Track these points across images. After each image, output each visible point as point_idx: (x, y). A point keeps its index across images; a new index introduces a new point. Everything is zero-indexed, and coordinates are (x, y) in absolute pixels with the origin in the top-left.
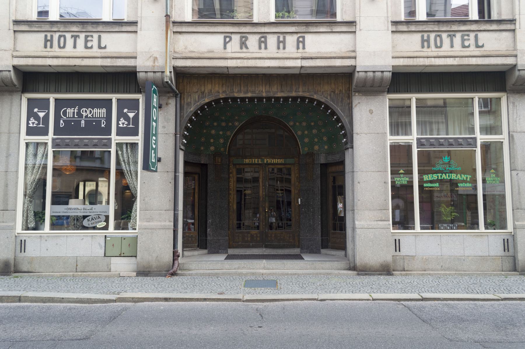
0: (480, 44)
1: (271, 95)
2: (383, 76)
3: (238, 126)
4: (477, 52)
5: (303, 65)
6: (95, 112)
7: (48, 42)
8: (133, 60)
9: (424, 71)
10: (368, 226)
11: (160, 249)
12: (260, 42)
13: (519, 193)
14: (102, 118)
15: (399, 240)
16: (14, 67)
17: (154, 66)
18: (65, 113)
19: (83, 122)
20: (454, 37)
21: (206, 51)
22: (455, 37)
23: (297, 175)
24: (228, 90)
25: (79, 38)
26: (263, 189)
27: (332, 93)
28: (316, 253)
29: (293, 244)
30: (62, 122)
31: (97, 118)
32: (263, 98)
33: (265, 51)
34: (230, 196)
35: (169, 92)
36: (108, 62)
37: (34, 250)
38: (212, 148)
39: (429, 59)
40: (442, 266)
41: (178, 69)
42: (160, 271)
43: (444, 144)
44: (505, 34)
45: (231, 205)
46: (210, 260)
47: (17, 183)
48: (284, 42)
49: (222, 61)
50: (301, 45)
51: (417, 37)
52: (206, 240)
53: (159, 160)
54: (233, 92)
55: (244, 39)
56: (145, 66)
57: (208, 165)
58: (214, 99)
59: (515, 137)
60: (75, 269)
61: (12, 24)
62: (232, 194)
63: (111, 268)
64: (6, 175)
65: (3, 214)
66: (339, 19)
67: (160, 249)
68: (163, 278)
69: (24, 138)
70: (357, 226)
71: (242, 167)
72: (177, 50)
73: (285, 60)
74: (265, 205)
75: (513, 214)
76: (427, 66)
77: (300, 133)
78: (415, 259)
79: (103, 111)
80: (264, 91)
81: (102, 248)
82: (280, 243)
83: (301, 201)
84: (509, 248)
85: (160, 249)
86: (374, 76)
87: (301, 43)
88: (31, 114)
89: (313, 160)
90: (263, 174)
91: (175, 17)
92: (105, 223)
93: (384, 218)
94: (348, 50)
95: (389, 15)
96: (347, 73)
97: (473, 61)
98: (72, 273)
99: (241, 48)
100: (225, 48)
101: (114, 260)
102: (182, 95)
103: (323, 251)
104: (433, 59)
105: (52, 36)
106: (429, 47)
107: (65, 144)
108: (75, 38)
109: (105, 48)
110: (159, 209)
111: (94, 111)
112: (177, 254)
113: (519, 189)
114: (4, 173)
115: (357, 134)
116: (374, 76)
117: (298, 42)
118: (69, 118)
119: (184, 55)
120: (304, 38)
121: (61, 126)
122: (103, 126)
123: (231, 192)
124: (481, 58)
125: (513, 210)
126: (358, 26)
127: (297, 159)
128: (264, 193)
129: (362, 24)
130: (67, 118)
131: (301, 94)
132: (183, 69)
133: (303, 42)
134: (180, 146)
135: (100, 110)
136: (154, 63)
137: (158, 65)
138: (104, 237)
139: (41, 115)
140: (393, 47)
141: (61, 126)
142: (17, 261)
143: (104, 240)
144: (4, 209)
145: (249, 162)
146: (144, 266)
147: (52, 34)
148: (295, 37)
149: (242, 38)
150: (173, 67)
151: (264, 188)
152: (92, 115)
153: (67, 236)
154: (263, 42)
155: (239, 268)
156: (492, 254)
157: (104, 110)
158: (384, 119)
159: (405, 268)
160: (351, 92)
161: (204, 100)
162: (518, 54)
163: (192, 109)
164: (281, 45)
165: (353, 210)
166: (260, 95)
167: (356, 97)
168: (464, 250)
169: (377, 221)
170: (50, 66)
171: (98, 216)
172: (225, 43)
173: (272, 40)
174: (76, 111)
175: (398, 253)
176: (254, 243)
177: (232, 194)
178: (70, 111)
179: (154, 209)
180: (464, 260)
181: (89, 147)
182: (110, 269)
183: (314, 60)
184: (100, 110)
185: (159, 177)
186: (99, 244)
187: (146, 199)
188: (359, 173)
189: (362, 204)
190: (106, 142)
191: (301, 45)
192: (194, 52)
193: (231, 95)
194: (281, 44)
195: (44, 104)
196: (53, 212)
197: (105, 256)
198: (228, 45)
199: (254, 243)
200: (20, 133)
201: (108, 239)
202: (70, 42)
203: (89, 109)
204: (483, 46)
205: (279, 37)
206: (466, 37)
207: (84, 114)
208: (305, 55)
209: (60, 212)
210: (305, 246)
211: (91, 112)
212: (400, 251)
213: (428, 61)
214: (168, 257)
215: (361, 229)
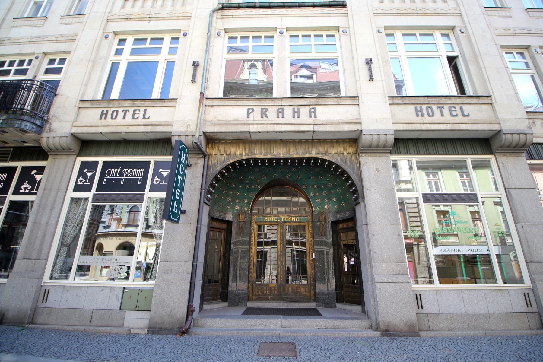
0: (466, 114)
1: (288, 156)
2: (387, 138)
4: (465, 119)
5: (315, 129)
7: (103, 115)
8: (169, 127)
9: (419, 138)
10: (388, 280)
11: (175, 303)
12: (278, 112)
13: (528, 246)
14: (139, 176)
15: (420, 295)
16: (72, 134)
17: (186, 131)
18: (109, 173)
19: (123, 180)
20: (442, 109)
21: (232, 119)
22: (444, 108)
23: (311, 231)
25: (129, 112)
26: (281, 244)
27: (341, 155)
28: (331, 307)
29: (308, 297)
30: (105, 180)
31: (136, 176)
32: (280, 159)
33: (283, 119)
34: (252, 250)
35: (199, 154)
36: (148, 129)
37: (55, 301)
38: (237, 207)
39: (424, 124)
40: (468, 325)
41: (208, 134)
42: (172, 328)
43: (448, 199)
44: (484, 106)
45: (251, 258)
46: (227, 315)
47: (54, 233)
48: (298, 112)
49: (245, 126)
50: (313, 114)
51: (411, 109)
52: (227, 292)
53: (184, 212)
55: (264, 110)
56: (179, 131)
57: (233, 222)
58: (238, 160)
59: (512, 193)
60: (89, 323)
61: (78, 102)
62: (253, 249)
63: (125, 322)
64: (47, 226)
65: (35, 263)
66: (343, 94)
67: (175, 303)
68: (174, 336)
69: (71, 194)
70: (376, 280)
71: (262, 224)
72: (207, 119)
73: (300, 125)
74: (282, 259)
75: (528, 267)
76: (424, 131)
77: (312, 195)
78: (440, 317)
79: (141, 171)
81: (119, 300)
83: (315, 255)
84: (531, 303)
85: (175, 303)
86: (379, 138)
87: (313, 113)
88: (81, 174)
89: (325, 218)
91: (209, 94)
92: (127, 274)
93: (402, 272)
94: (354, 118)
95: (386, 92)
96: (353, 139)
97: (464, 127)
98: (83, 328)
99: (262, 117)
100: (248, 117)
101: (128, 314)
102: (210, 157)
103: (339, 305)
104: (428, 125)
105: (107, 111)
106: (423, 116)
107: (103, 199)
108: (125, 111)
109: (148, 118)
110: (179, 260)
111: (134, 171)
112: (191, 309)
113: (527, 242)
114: (45, 224)
115: (367, 189)
116: (379, 138)
117: (310, 112)
118: (112, 176)
119: (213, 123)
120: (315, 109)
121: (104, 184)
122: (139, 183)
123: (252, 246)
124: (469, 124)
125: (526, 263)
126: (360, 100)
127: (311, 218)
129: (363, 98)
130: (110, 177)
131: (314, 156)
132: (211, 135)
133: (315, 112)
134: (204, 200)
135: (139, 170)
136: (187, 128)
137: (190, 130)
138: (122, 289)
139: (89, 174)
140: (392, 116)
141: (104, 184)
142: (37, 311)
143: (122, 292)
144: (37, 258)
146: (156, 322)
147: (107, 109)
148: (308, 108)
149: (262, 109)
150: (204, 133)
152: (132, 175)
153: (88, 286)
154: (280, 112)
155: (255, 325)
156: (516, 310)
158: (391, 177)
159: (431, 328)
160: (357, 154)
162: (500, 121)
163: (217, 169)
164: (296, 114)
165: (371, 263)
166: (277, 157)
167: (363, 158)
168: (487, 306)
169: (395, 274)
170: (101, 133)
171: (121, 267)
172: (249, 114)
173: (288, 111)
174: (118, 171)
175: (420, 310)
177: (253, 249)
178: (113, 171)
179: (174, 261)
180: (490, 317)
181: (124, 201)
182: (123, 324)
183: (325, 125)
184: (139, 170)
185: (182, 229)
186: (117, 295)
187: (167, 250)
188: (373, 225)
189: (379, 257)
190: (139, 197)
191: (313, 114)
193: (253, 157)
194: (296, 113)
196: (81, 262)
197: (120, 309)
198: (251, 115)
200: (67, 189)
201: (126, 291)
202: (121, 114)
203: (130, 169)
204: (468, 116)
205: (294, 109)
206: (453, 109)
207: (125, 173)
208: (316, 122)
209: (87, 263)
211: (131, 171)
212: (422, 308)
213: (425, 127)
214: (182, 311)
215: (380, 283)
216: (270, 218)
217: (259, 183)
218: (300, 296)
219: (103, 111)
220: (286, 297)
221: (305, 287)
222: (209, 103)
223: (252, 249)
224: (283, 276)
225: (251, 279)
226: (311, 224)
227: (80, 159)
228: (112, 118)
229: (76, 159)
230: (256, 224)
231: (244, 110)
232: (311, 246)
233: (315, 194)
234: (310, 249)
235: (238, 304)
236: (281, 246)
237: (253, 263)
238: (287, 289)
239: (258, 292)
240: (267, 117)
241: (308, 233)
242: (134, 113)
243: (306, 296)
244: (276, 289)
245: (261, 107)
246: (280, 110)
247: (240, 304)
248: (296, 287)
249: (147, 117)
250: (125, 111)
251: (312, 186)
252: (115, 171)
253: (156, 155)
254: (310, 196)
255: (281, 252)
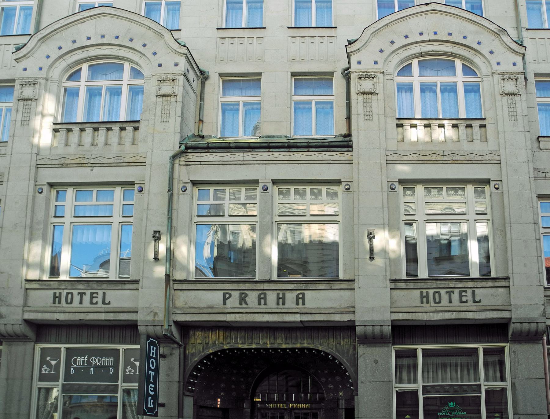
6: (104, 361)
12: (260, 298)
14: (110, 366)
19: (92, 370)
21: (206, 306)
24: (232, 342)
30: (72, 369)
31: (106, 366)
33: (265, 306)
48: (284, 298)
50: (300, 301)
54: (238, 343)
55: (243, 295)
80: (268, 342)
88: (43, 362)
99: (241, 304)
100: (225, 303)
108: (82, 295)
109: (109, 303)
111: (103, 360)
117: (298, 298)
118: (79, 365)
120: (303, 294)
121: (71, 373)
122: (110, 373)
130: (77, 366)
135: (108, 359)
139: (53, 363)
148: (295, 293)
154: (262, 298)
157: (112, 359)
161: (209, 351)
172: (225, 300)
173: (272, 297)
174: (85, 359)
184: (108, 359)
191: (300, 301)
192: (194, 307)
195: (56, 353)
198: (228, 301)
202: (77, 298)
203: (98, 358)
205: (278, 294)
207: (93, 362)
219: (55, 293)
222: (176, 286)
227: (38, 347)
228: (67, 303)
229: (34, 346)
231: (220, 295)
240: (247, 304)
242: (92, 298)
245: (239, 292)
246: (262, 296)
249: (107, 301)
250: (82, 295)
252: (82, 359)
253: (125, 343)
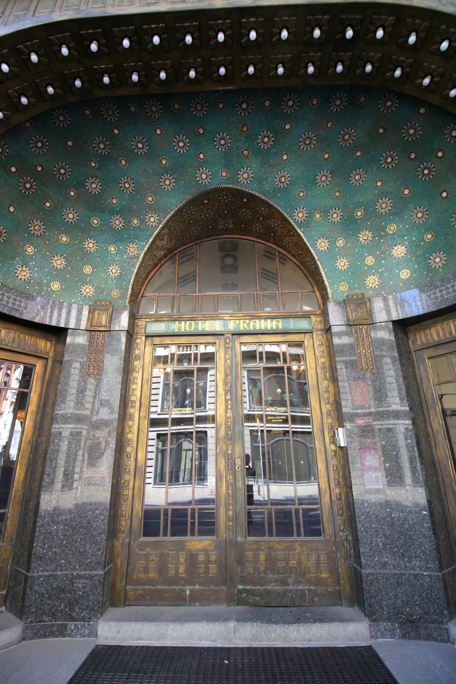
3: (157, 227)
23: (323, 360)
26: (226, 401)
28: (429, 637)
29: (330, 589)
34: (130, 423)
45: (129, 449)
57: (69, 330)
74: (233, 450)
82: (288, 585)
90: (226, 360)
128: (229, 414)
145: (188, 329)
151: (228, 397)
176: (197, 587)
199: (197, 587)
210: (382, 608)
216: (193, 322)
217: (153, 209)
218: (299, 583)
220: (248, 587)
221: (317, 550)
223: (131, 419)
224: (235, 511)
225: (124, 523)
226: (320, 337)
230: (148, 342)
232: (328, 406)
233: (332, 243)
234: (325, 416)
235: (65, 626)
236: (227, 407)
237: (132, 468)
238: (249, 554)
239: (146, 570)
241: (313, 365)
243: (318, 582)
244: (213, 558)
247: (71, 625)
248: (283, 550)
251: (325, 212)
254: (315, 249)
255: (228, 428)
